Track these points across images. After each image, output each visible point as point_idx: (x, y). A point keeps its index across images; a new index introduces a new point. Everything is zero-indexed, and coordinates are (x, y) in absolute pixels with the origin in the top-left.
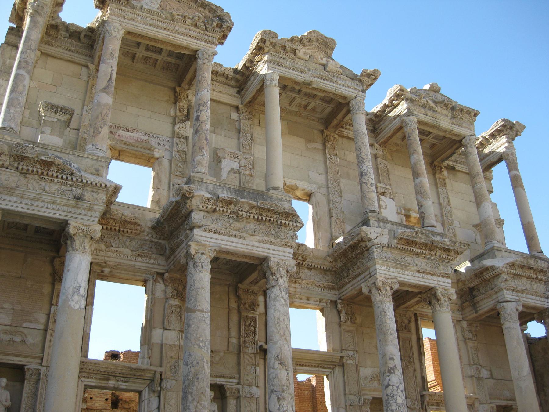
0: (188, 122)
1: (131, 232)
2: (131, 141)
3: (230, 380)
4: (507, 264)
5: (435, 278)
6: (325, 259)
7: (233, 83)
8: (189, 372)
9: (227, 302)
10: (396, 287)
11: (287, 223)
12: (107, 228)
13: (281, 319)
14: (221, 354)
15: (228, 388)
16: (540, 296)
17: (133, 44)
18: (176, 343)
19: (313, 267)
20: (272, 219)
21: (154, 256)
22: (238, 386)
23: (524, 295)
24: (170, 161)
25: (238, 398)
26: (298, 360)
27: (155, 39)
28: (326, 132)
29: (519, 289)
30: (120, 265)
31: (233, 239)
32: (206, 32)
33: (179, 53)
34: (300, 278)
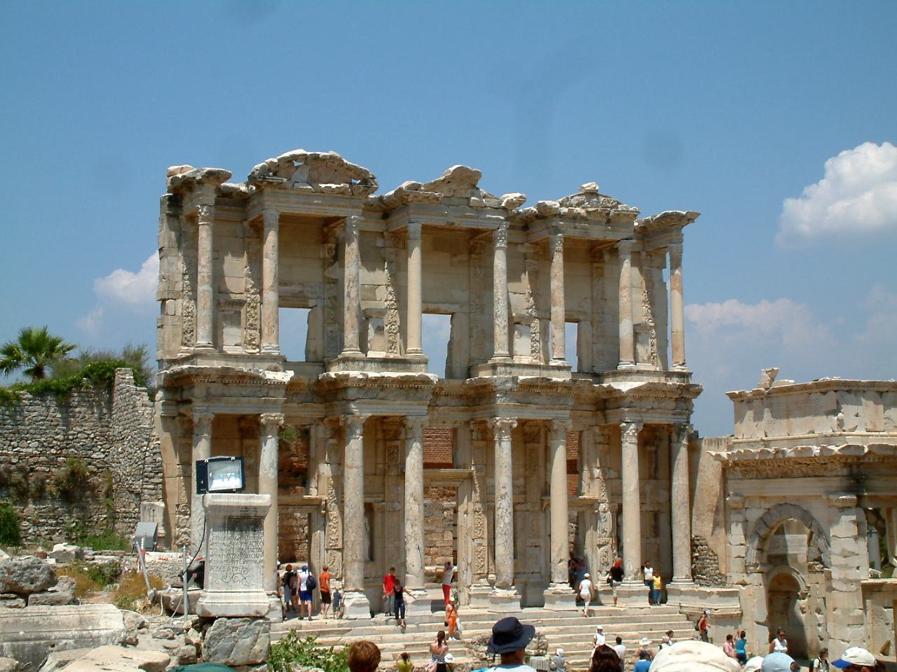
0: (337, 263)
3: (377, 499)
5: (555, 412)
7: (378, 209)
8: (350, 512)
10: (515, 425)
16: (667, 414)
17: (287, 223)
21: (315, 405)
22: (384, 503)
24: (323, 308)
25: (383, 512)
29: (644, 410)
31: (380, 406)
32: (354, 197)
34: (437, 406)
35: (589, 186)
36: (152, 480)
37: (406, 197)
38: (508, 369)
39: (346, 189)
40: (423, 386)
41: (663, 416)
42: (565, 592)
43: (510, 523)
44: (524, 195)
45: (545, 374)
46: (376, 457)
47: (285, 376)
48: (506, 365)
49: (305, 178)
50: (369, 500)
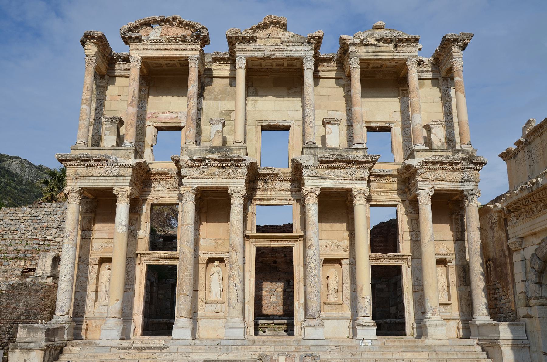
2: (167, 120)
4: (420, 162)
5: (353, 182)
10: (319, 192)
13: (235, 223)
23: (438, 183)
35: (379, 23)
36: (56, 239)
37: (231, 40)
38: (313, 151)
39: (185, 37)
41: (452, 183)
42: (366, 324)
43: (315, 268)
44: (321, 31)
45: (343, 154)
47: (133, 161)
48: (311, 148)
49: (159, 34)
50: (221, 256)
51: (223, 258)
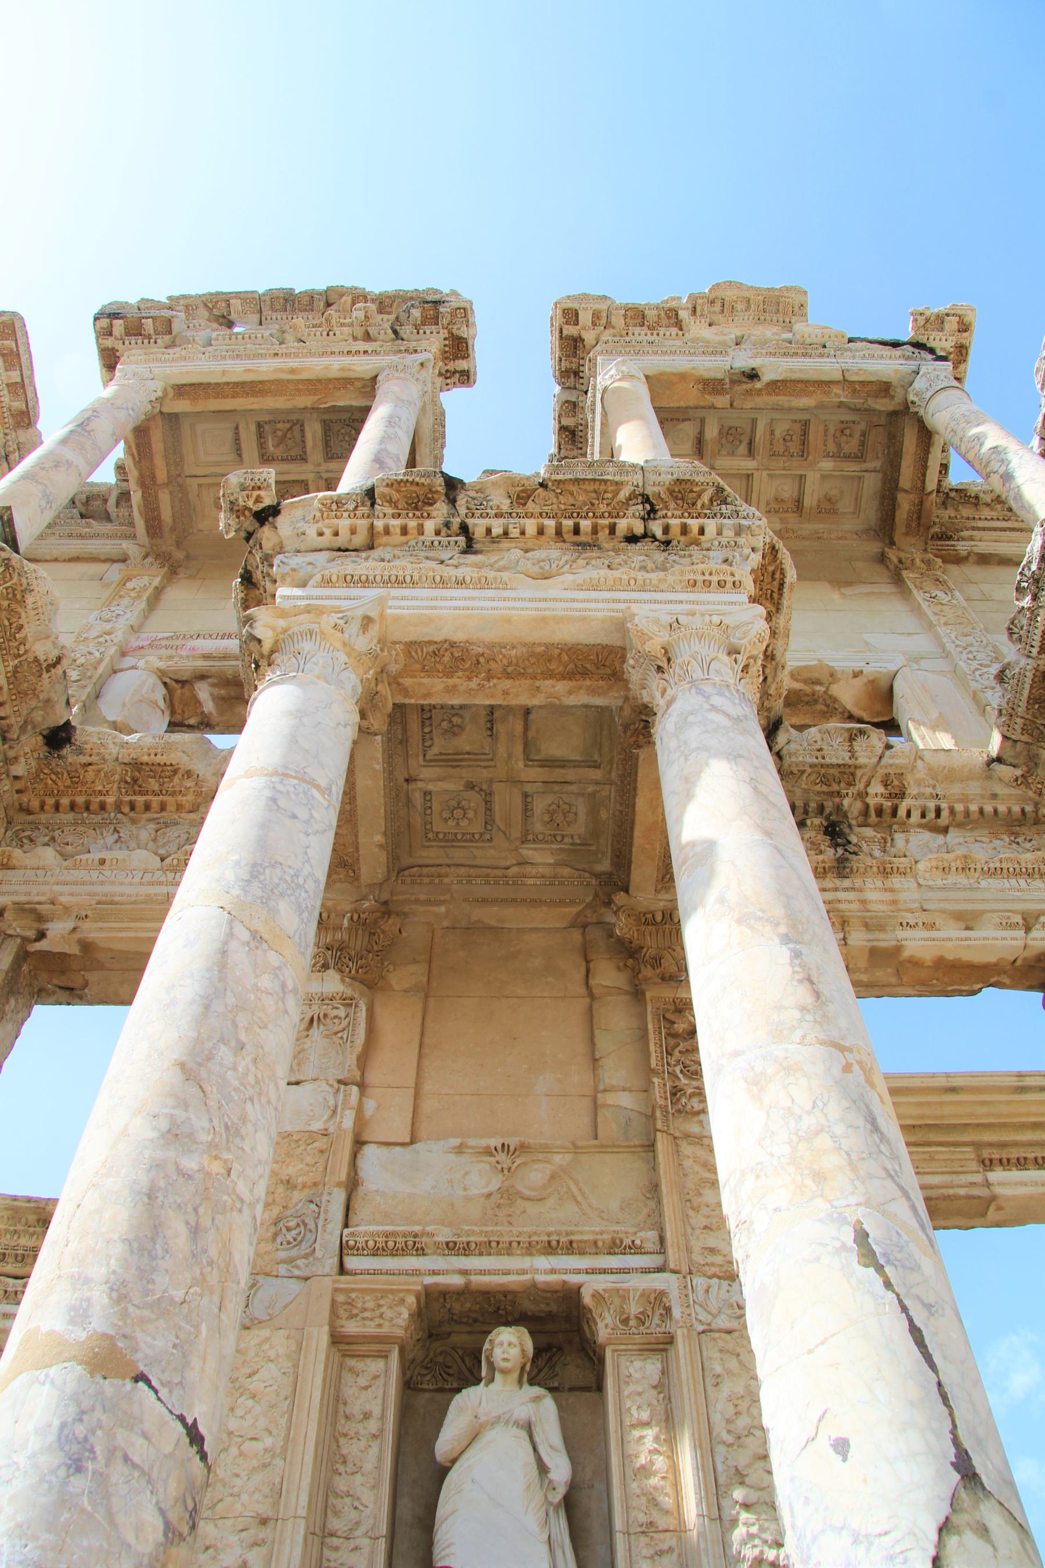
1: (163, 807)
6: (989, 778)
9: (579, 976)
11: (694, 524)
12: (73, 806)
14: (557, 1158)
15: (597, 1296)
18: (317, 1126)
19: (945, 814)
20: (622, 525)
25: (664, 1345)
26: (987, 1137)
27: (253, 384)
28: (892, 555)
30: (112, 903)
33: (334, 409)
37: (570, 330)
40: (694, 524)
46: (595, 1061)
51: (570, 1296)
